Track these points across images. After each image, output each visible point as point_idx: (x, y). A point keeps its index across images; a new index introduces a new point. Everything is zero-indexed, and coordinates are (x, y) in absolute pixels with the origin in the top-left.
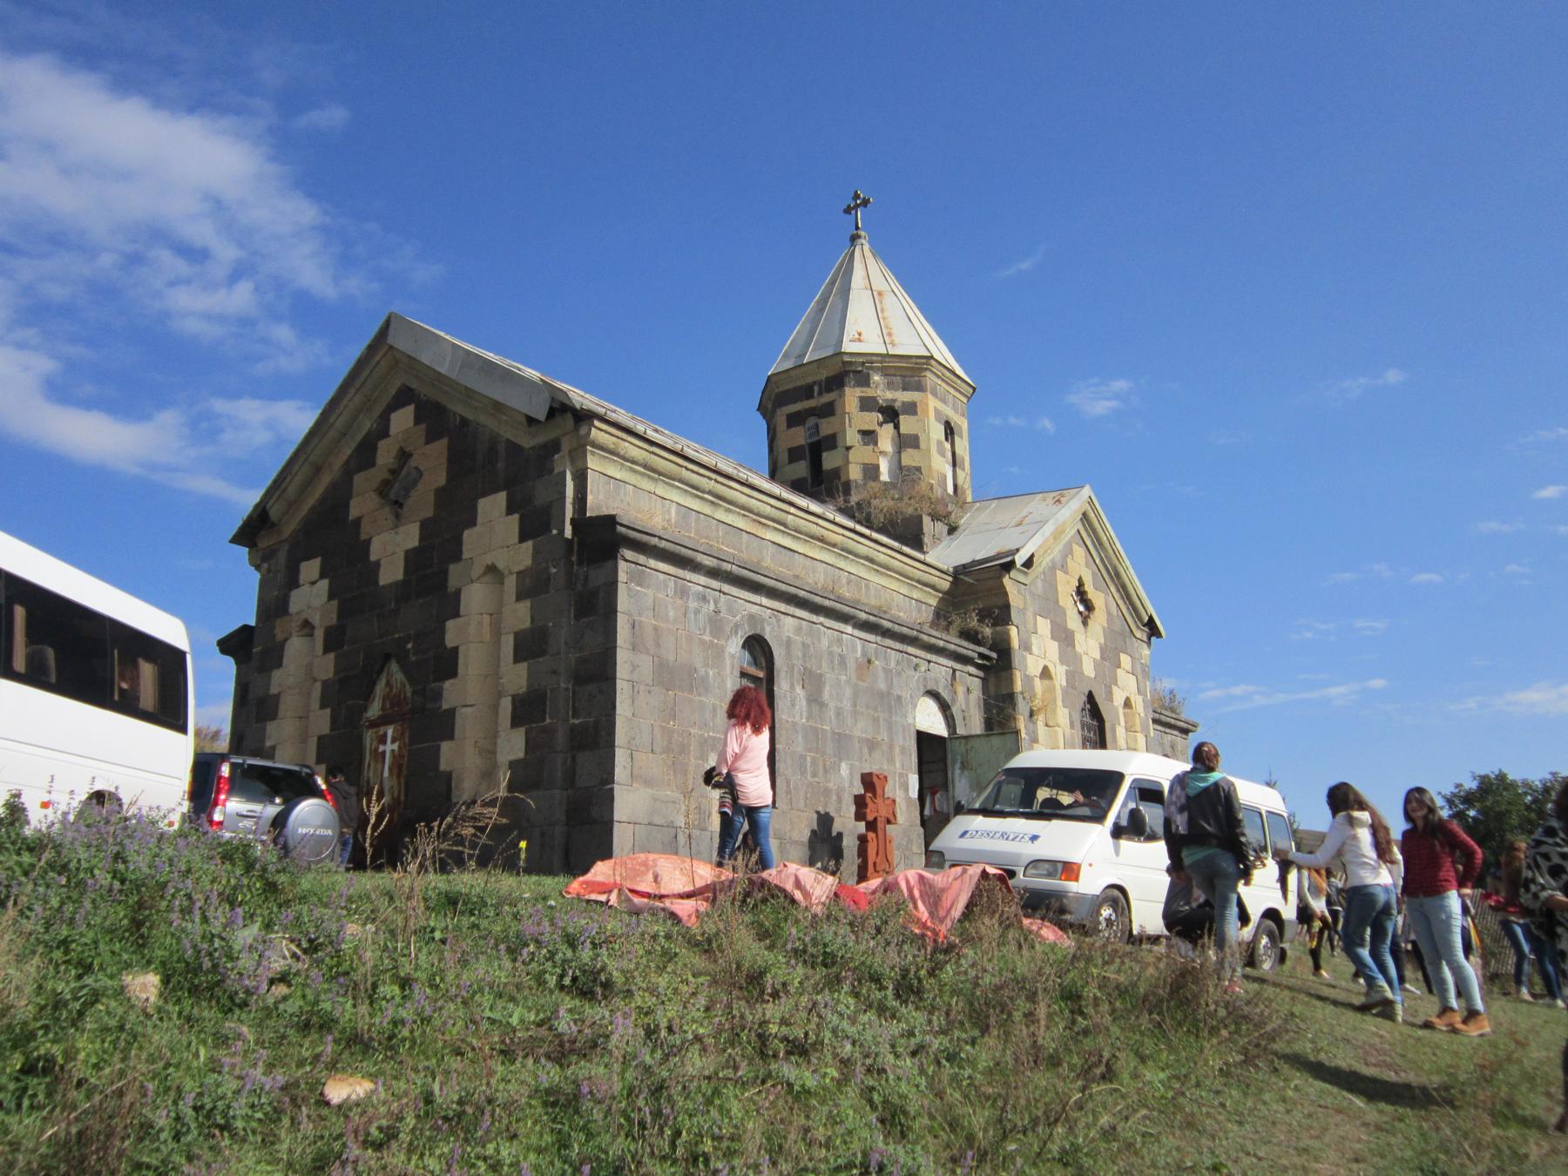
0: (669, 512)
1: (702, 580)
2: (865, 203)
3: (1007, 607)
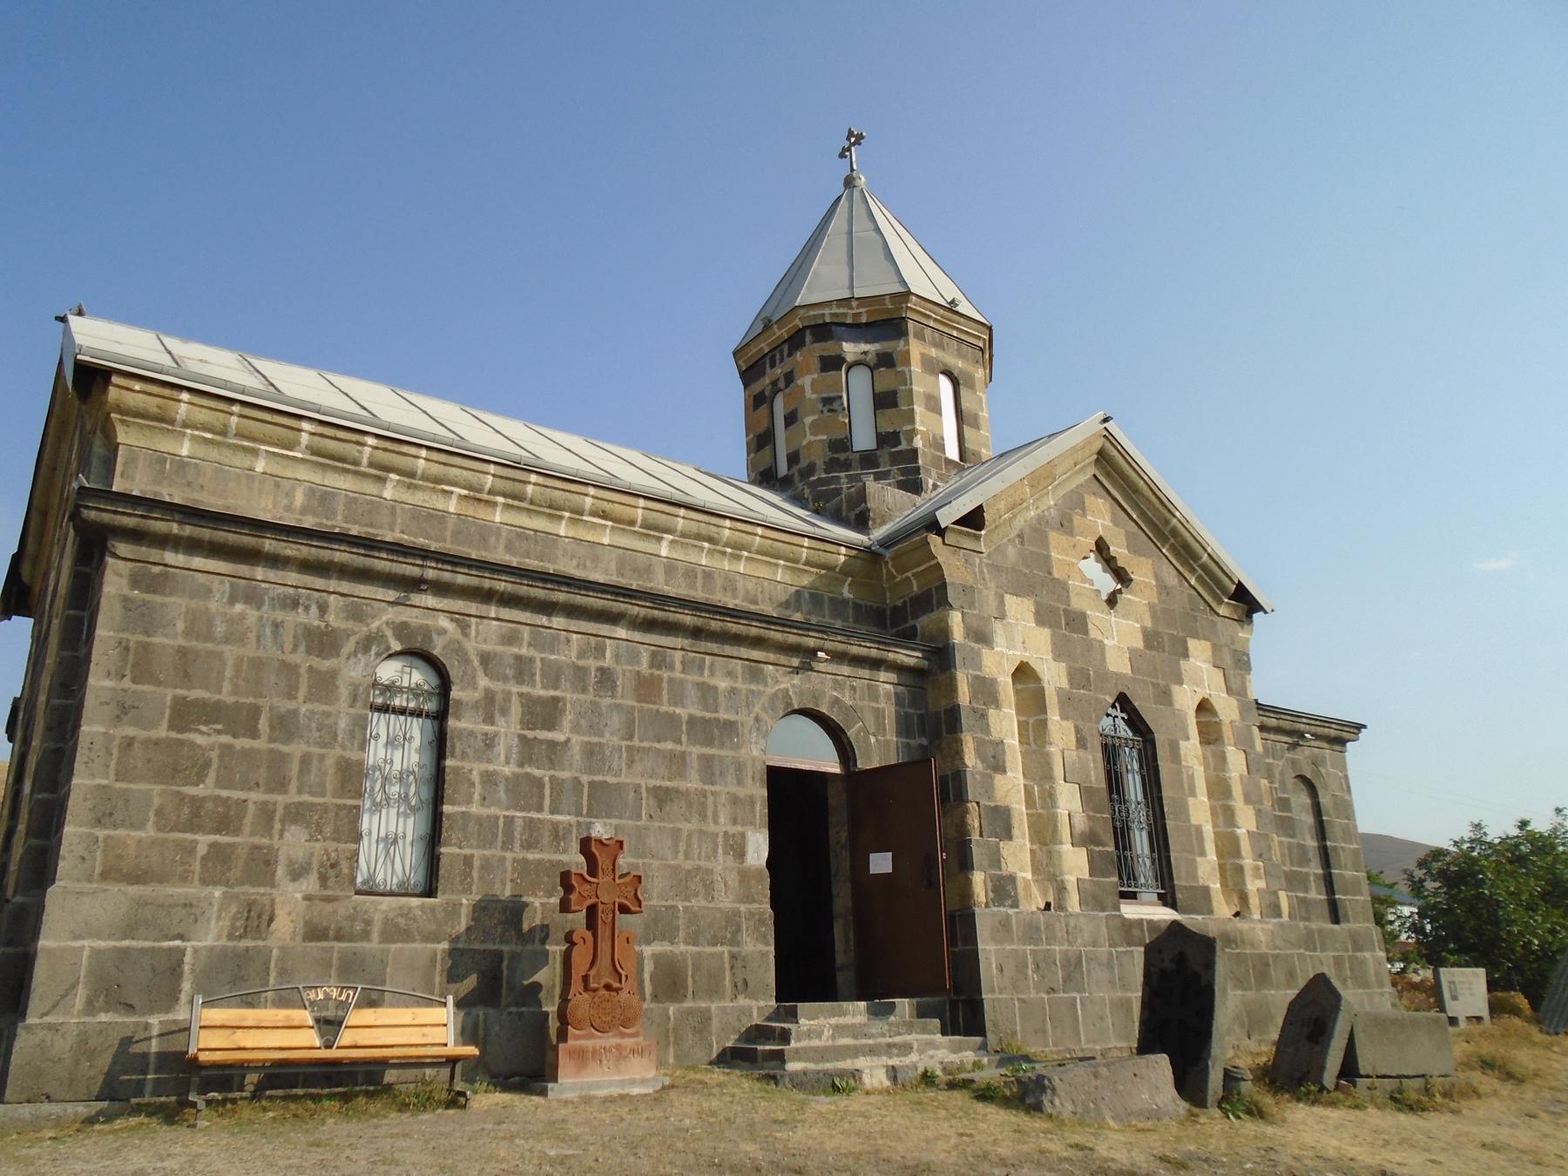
0: (290, 494)
1: (293, 577)
2: (860, 137)
3: (943, 586)
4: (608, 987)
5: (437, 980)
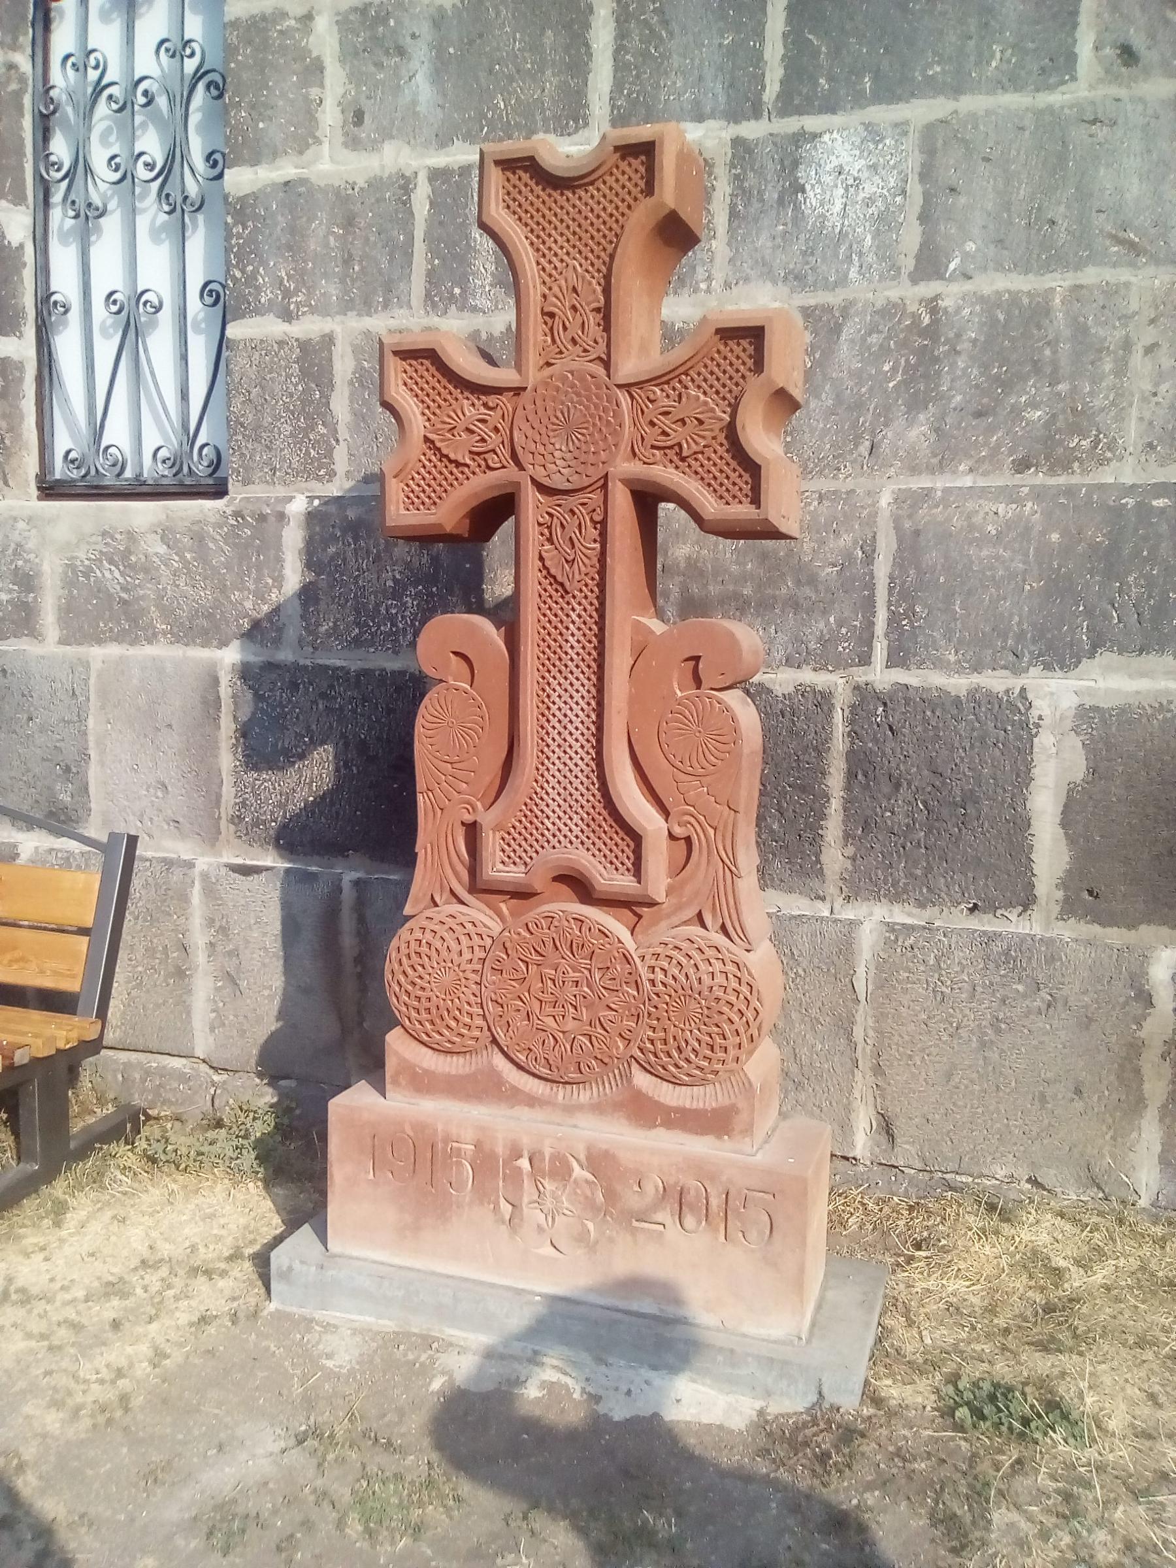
4: (577, 884)
5: (227, 760)
